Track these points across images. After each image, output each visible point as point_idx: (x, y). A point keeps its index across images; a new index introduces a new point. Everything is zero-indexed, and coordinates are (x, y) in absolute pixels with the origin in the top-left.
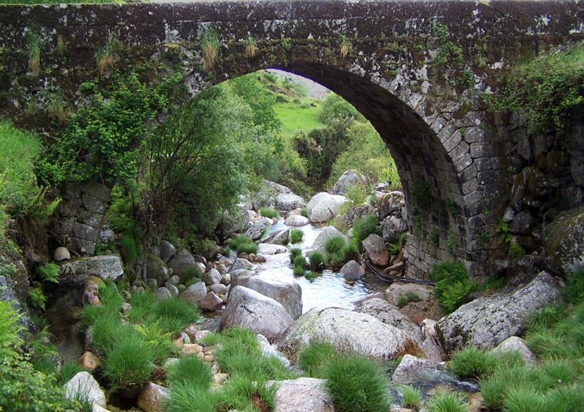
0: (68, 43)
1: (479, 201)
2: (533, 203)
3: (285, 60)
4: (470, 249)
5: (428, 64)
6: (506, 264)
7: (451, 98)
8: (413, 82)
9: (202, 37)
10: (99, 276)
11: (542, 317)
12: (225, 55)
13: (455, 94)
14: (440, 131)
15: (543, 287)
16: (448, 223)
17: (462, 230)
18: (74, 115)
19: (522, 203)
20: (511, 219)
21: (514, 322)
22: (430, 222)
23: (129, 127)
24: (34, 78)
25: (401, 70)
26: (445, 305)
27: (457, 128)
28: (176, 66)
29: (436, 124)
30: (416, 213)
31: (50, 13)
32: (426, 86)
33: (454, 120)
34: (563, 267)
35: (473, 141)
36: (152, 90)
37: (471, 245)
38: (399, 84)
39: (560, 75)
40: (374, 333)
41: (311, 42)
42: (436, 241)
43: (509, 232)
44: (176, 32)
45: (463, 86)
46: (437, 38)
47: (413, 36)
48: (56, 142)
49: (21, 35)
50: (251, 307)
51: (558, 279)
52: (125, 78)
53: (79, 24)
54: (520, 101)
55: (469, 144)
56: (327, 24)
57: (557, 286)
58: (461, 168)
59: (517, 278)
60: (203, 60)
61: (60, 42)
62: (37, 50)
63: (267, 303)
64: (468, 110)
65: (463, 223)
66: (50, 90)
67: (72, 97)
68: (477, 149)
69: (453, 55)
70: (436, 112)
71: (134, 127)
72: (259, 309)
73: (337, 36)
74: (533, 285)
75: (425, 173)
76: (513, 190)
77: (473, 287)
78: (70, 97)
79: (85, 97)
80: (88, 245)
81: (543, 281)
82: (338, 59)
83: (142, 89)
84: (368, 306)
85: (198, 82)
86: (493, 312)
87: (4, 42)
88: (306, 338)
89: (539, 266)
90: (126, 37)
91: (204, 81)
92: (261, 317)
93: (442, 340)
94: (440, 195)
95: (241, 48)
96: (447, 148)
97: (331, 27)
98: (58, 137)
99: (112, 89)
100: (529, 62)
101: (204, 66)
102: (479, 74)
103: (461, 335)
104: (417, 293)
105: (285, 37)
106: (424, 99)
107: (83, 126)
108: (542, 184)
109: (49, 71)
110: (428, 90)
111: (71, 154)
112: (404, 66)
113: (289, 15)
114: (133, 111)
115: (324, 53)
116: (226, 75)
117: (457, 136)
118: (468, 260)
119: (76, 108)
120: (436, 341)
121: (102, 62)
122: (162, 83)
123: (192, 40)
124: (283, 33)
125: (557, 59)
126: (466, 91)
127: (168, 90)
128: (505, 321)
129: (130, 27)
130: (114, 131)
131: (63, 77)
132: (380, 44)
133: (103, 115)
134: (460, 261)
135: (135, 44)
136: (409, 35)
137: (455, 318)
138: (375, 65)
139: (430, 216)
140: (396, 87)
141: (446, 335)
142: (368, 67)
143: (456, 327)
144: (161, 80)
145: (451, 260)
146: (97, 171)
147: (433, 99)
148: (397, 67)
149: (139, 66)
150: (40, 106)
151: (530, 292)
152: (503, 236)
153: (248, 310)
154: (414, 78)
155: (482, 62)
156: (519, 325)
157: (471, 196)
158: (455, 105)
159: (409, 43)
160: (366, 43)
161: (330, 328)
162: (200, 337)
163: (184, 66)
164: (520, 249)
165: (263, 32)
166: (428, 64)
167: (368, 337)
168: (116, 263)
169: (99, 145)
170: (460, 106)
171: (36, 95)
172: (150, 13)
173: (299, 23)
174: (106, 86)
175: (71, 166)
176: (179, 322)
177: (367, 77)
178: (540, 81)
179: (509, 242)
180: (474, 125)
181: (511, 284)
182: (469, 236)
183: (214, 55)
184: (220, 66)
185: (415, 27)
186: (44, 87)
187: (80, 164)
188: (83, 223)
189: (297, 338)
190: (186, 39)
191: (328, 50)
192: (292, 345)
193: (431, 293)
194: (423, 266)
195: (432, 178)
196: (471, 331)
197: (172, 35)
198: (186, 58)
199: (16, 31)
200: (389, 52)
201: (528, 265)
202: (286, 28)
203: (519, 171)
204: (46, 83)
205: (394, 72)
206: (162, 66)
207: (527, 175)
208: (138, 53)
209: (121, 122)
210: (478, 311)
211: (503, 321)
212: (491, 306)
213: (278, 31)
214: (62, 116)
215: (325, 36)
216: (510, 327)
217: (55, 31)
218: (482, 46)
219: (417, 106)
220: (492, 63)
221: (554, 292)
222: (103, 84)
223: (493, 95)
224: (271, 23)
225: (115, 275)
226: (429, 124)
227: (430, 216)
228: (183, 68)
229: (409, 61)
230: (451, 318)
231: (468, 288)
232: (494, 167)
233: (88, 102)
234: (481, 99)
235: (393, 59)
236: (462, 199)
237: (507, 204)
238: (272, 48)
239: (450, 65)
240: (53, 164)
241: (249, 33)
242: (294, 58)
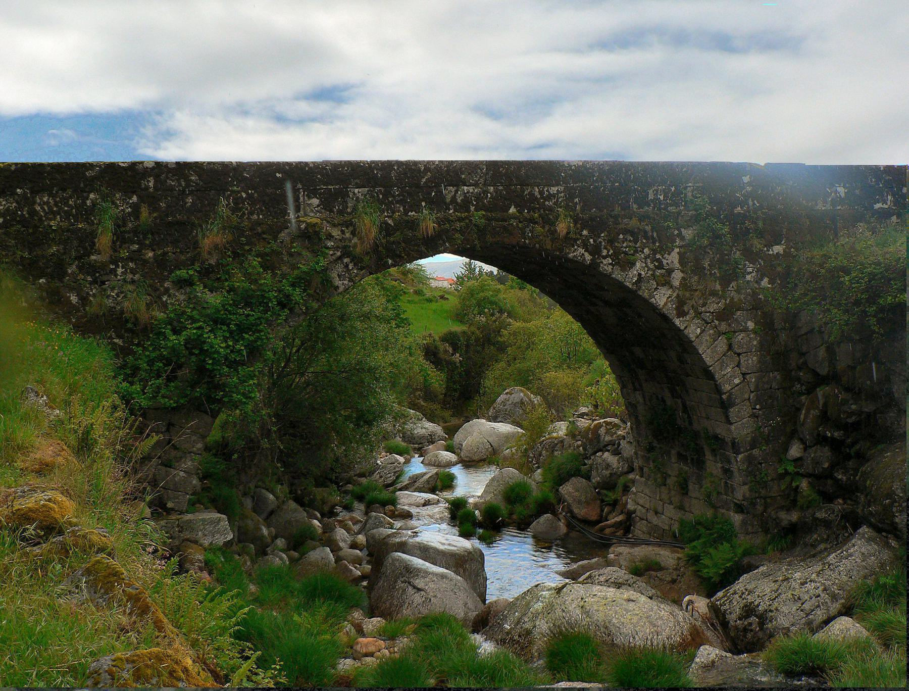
0: (155, 215)
1: (752, 432)
2: (836, 434)
3: (476, 242)
4: (741, 498)
5: (680, 247)
6: (794, 517)
7: (714, 293)
8: (658, 272)
9: (355, 209)
10: (196, 542)
11: (876, 589)
12: (388, 234)
13: (718, 287)
14: (697, 337)
15: (869, 547)
16: (704, 462)
17: (727, 472)
18: (161, 316)
19: (818, 435)
20: (798, 455)
21: (834, 597)
22: (673, 460)
23: (246, 333)
24: (102, 262)
25: (643, 256)
26: (705, 576)
27: (720, 334)
28: (316, 247)
29: (692, 330)
30: (651, 449)
31: (129, 173)
32: (677, 277)
33: (717, 322)
34: (897, 520)
35: (744, 350)
36: (281, 282)
37: (741, 492)
38: (640, 275)
39: (875, 264)
40: (647, 618)
41: (513, 217)
42: (684, 488)
43: (798, 474)
44: (315, 201)
45: (730, 276)
46: (694, 212)
47: (659, 209)
48: (133, 353)
49: (84, 203)
50: (419, 583)
51: (887, 537)
52: (241, 265)
53: (171, 189)
54: (814, 298)
55: (739, 355)
56: (537, 194)
57: (887, 545)
58: (727, 387)
59: (815, 536)
60: (355, 240)
61: (144, 213)
62: (109, 224)
63: (443, 576)
64: (738, 310)
65: (729, 462)
66: (125, 280)
67: (158, 289)
68: (750, 362)
69: (717, 236)
70: (691, 311)
71: (254, 333)
72: (432, 585)
73: (551, 209)
74: (854, 546)
75: (667, 395)
76: (802, 417)
77: (745, 550)
78: (156, 290)
79: (178, 290)
80: (177, 498)
81: (870, 540)
82: (552, 241)
83: (267, 279)
84: (602, 579)
85: (348, 270)
86: (802, 584)
87: (59, 214)
88: (543, 626)
89: (853, 522)
90: (242, 208)
91: (358, 269)
92: (435, 596)
93: (725, 624)
94: (691, 424)
95: (413, 225)
96: (708, 360)
97: (542, 197)
98: (138, 345)
99: (219, 279)
100: (822, 246)
101: (358, 250)
102: (753, 262)
103: (756, 616)
104: (658, 559)
105: (476, 210)
106: (675, 295)
107: (175, 332)
108: (850, 408)
109: (124, 254)
110: (681, 283)
111: (158, 370)
112: (646, 250)
113: (482, 180)
114: (251, 310)
115: (532, 232)
116: (390, 262)
117: (721, 344)
118: (736, 512)
119: (165, 306)
120: (712, 625)
121: (206, 243)
122: (296, 272)
123: (341, 212)
124: (473, 205)
125: (869, 243)
126: (733, 284)
127: (303, 282)
128: (822, 595)
129: (247, 194)
130: (225, 339)
131: (145, 262)
132: (612, 220)
133: (208, 316)
134: (723, 514)
135: (255, 217)
136: (654, 208)
137: (743, 594)
138: (605, 248)
139: (673, 452)
140: (635, 279)
141: (732, 618)
142: (595, 251)
143: (746, 606)
144: (294, 267)
145: (709, 513)
146: (197, 394)
147: (688, 294)
148: (636, 251)
149: (259, 248)
150: (109, 302)
151: (851, 555)
152: (788, 479)
153: (414, 587)
154: (660, 266)
155: (757, 244)
156: (843, 601)
157: (742, 425)
158: (718, 303)
159: (654, 220)
160: (592, 219)
161: (578, 611)
162: (370, 626)
163: (327, 248)
164: (815, 496)
165: (445, 203)
166: (680, 247)
167: (637, 623)
168: (222, 523)
169: (202, 357)
170: (725, 304)
171: (104, 287)
172: (278, 175)
173: (496, 191)
174: (211, 275)
175: (159, 388)
176: (340, 607)
177: (594, 265)
178: (847, 271)
179: (797, 487)
180: (745, 330)
181: (805, 545)
182: (738, 478)
183: (374, 231)
184: (380, 249)
185: (662, 198)
186: (116, 275)
187: (172, 384)
188: (170, 467)
189: (528, 626)
190: (331, 211)
191: (539, 229)
192: (520, 636)
193: (679, 559)
194: (662, 522)
195: (679, 401)
196: (771, 611)
197: (309, 205)
198: (330, 237)
199: (78, 199)
200: (626, 232)
201: (832, 517)
202: (478, 198)
203: (810, 391)
204: (120, 271)
205: (632, 258)
206: (296, 247)
207: (823, 395)
208: (260, 230)
209: (235, 325)
210: (779, 583)
211: (819, 596)
212: (797, 575)
213: (467, 202)
214: (144, 317)
215: (534, 209)
216: (829, 604)
217: (135, 198)
218: (756, 223)
219: (666, 304)
220: (769, 246)
221: (886, 555)
222: (206, 272)
223: (773, 289)
224: (456, 192)
225: (220, 540)
226: (682, 328)
227: (673, 452)
228: (327, 251)
229: (654, 243)
230: (735, 593)
231: (740, 551)
232: (774, 385)
233: (182, 297)
234: (754, 294)
235: (630, 241)
236: (729, 430)
237: (793, 435)
238: (458, 225)
239: (711, 249)
240: (132, 384)
241: (423, 204)
242: (489, 239)
